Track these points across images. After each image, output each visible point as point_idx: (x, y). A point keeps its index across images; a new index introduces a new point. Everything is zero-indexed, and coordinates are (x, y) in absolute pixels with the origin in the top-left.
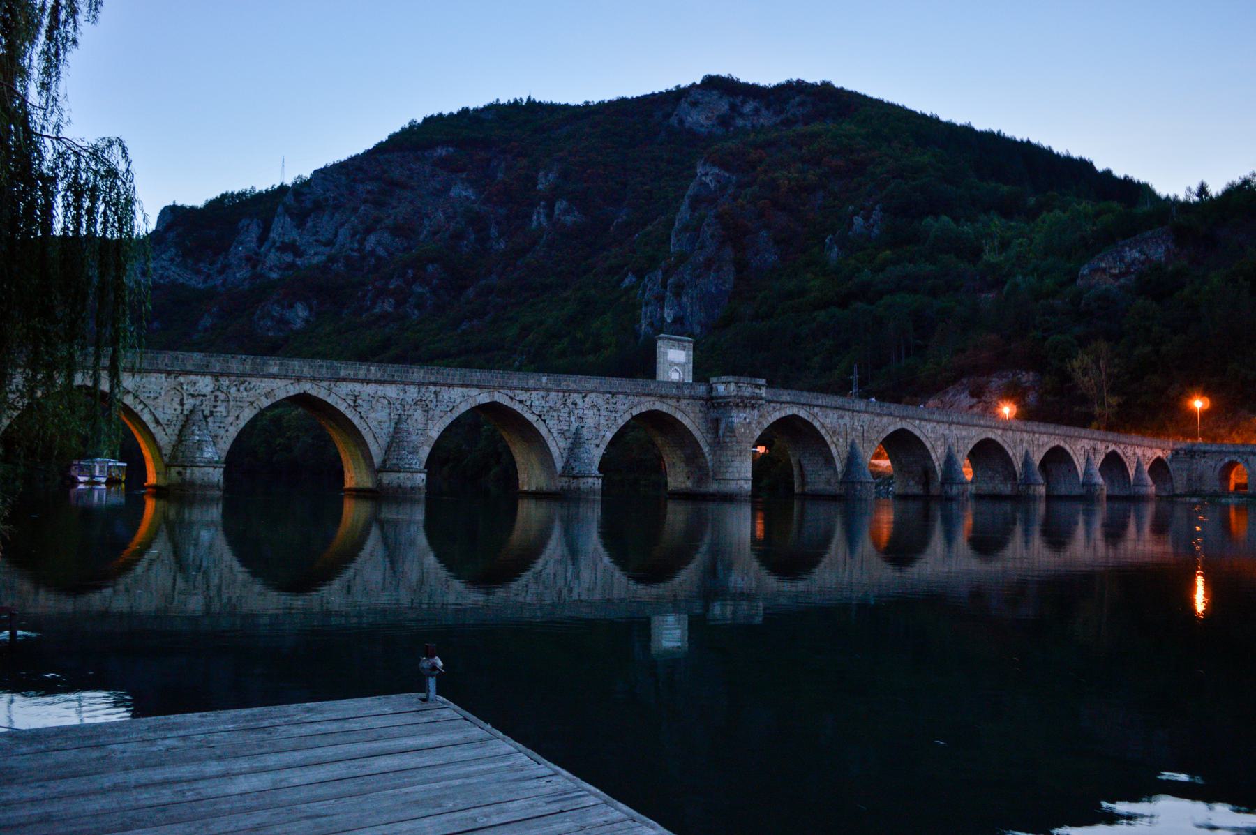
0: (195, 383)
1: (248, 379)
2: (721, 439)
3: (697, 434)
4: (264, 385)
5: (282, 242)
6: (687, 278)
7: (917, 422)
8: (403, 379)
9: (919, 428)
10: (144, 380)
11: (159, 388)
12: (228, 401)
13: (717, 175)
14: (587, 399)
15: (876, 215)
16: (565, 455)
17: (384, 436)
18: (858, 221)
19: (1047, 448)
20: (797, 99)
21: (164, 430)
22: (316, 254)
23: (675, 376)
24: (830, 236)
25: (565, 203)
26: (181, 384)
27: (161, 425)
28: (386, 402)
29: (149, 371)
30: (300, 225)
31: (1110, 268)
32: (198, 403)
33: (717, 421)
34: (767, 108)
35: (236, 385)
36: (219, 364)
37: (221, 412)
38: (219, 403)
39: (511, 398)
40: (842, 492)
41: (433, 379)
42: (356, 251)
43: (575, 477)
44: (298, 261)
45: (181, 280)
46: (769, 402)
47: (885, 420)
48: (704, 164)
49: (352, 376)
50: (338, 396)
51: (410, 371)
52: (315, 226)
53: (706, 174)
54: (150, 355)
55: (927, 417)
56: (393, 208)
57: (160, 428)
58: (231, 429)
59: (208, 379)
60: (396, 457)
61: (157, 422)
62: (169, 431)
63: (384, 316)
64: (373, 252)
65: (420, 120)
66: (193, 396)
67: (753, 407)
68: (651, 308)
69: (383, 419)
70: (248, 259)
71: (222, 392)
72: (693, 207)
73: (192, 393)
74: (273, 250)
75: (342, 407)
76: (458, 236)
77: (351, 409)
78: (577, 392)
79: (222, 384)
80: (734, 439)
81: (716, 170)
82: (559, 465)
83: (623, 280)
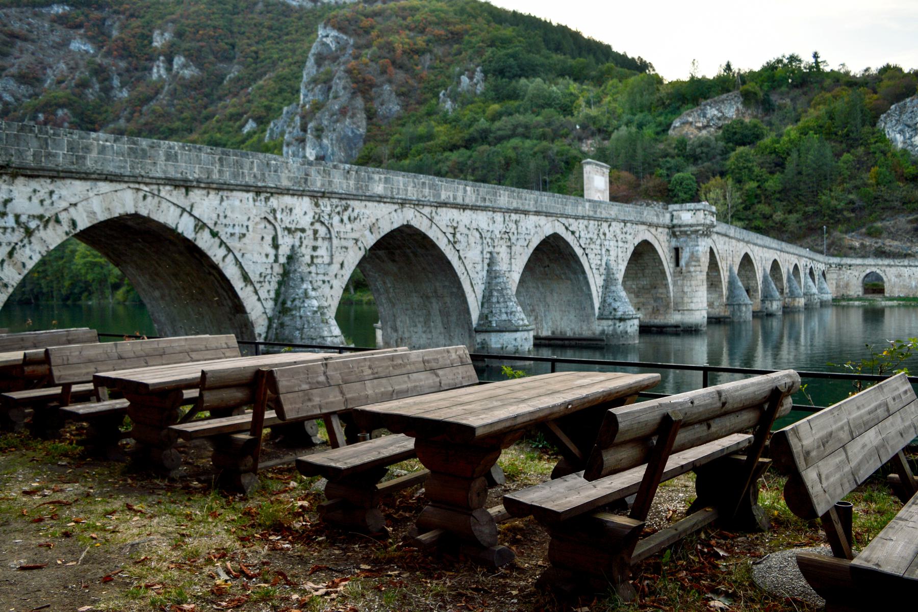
0: (291, 210)
1: (351, 203)
4: (367, 212)
6: (326, 123)
7: (752, 246)
10: (225, 204)
11: (246, 218)
12: (330, 238)
13: (337, 37)
15: (478, 76)
16: (600, 294)
18: (465, 79)
21: (256, 292)
24: (443, 92)
25: (183, 59)
26: (274, 211)
27: (252, 283)
28: (478, 235)
29: (231, 188)
32: (297, 244)
33: (677, 250)
35: (339, 213)
37: (322, 257)
38: (319, 243)
39: (567, 229)
40: (727, 314)
43: (621, 320)
47: (741, 244)
48: (325, 27)
49: (451, 200)
53: (327, 36)
54: (233, 158)
56: (15, 58)
57: (250, 289)
60: (503, 310)
61: (246, 278)
62: (263, 294)
66: (289, 230)
71: (323, 223)
73: (289, 226)
76: (84, 85)
77: (451, 246)
79: (323, 211)
81: (334, 33)
83: (243, 126)
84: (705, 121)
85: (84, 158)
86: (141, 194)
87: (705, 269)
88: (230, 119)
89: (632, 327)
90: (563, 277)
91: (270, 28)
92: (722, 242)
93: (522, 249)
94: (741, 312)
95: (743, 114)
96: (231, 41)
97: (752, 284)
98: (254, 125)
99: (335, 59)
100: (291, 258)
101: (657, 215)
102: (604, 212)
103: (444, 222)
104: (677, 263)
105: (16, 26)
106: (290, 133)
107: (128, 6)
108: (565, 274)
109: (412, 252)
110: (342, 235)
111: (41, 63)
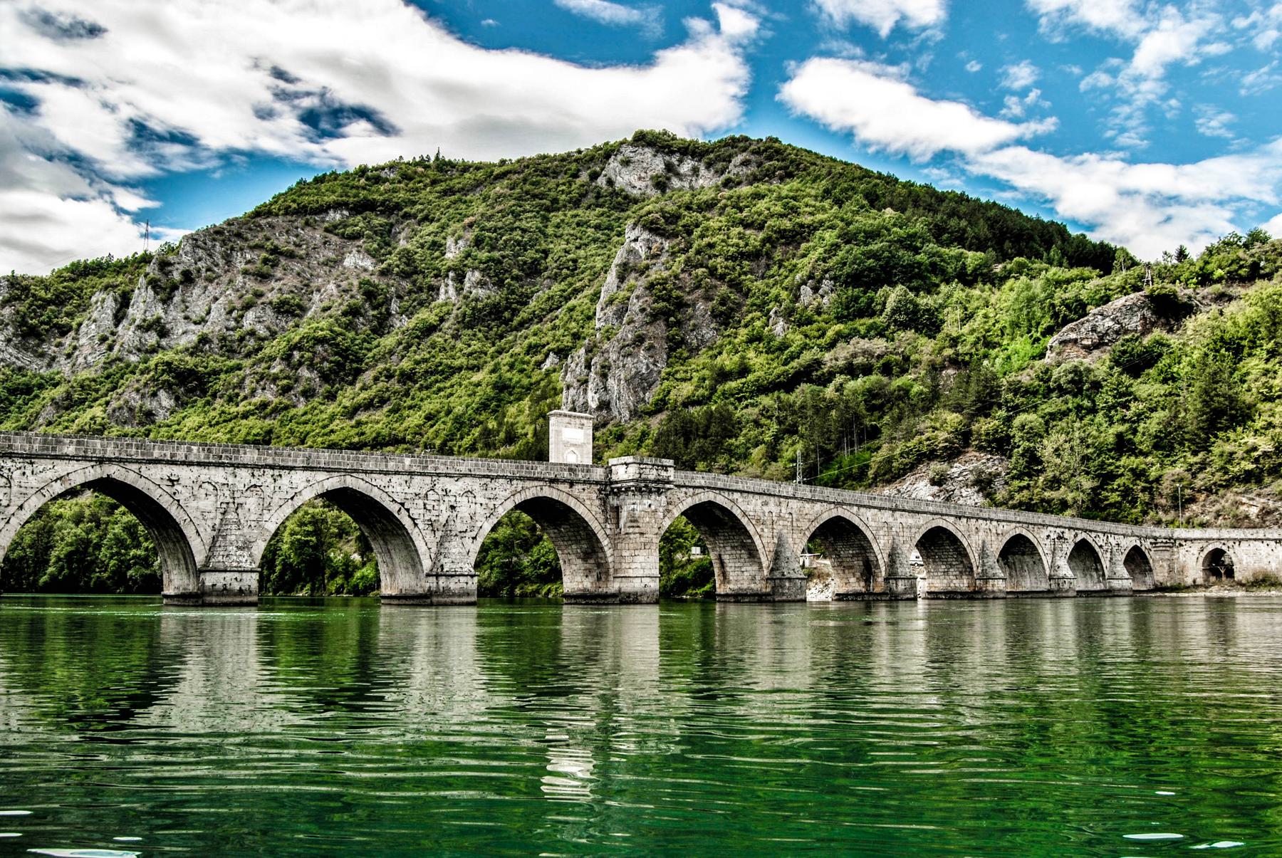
3: (595, 526)
5: (144, 320)
6: (613, 356)
8: (233, 461)
9: (857, 515)
14: (460, 483)
17: (209, 530)
18: (806, 290)
19: (1008, 537)
20: (739, 158)
22: (184, 333)
23: (572, 459)
25: (477, 274)
30: (166, 301)
31: (1082, 339)
33: (617, 510)
34: (709, 166)
41: (270, 461)
42: (233, 329)
44: (164, 342)
45: (19, 363)
46: (679, 486)
47: (818, 506)
50: (151, 480)
51: (242, 451)
52: (183, 301)
53: (636, 240)
55: (866, 503)
58: (13, 520)
63: (264, 405)
64: (252, 333)
65: (310, 180)
67: (660, 494)
68: (572, 391)
69: (208, 509)
70: (103, 339)
72: (622, 278)
74: (132, 328)
75: (155, 494)
76: (353, 312)
78: (446, 475)
80: (637, 530)
81: (646, 235)
82: (427, 564)
84: (1095, 336)
88: (527, 353)
91: (597, 227)
96: (544, 246)
98: (557, 360)
99: (643, 271)
105: (281, 241)
107: (420, 207)
111: (307, 285)
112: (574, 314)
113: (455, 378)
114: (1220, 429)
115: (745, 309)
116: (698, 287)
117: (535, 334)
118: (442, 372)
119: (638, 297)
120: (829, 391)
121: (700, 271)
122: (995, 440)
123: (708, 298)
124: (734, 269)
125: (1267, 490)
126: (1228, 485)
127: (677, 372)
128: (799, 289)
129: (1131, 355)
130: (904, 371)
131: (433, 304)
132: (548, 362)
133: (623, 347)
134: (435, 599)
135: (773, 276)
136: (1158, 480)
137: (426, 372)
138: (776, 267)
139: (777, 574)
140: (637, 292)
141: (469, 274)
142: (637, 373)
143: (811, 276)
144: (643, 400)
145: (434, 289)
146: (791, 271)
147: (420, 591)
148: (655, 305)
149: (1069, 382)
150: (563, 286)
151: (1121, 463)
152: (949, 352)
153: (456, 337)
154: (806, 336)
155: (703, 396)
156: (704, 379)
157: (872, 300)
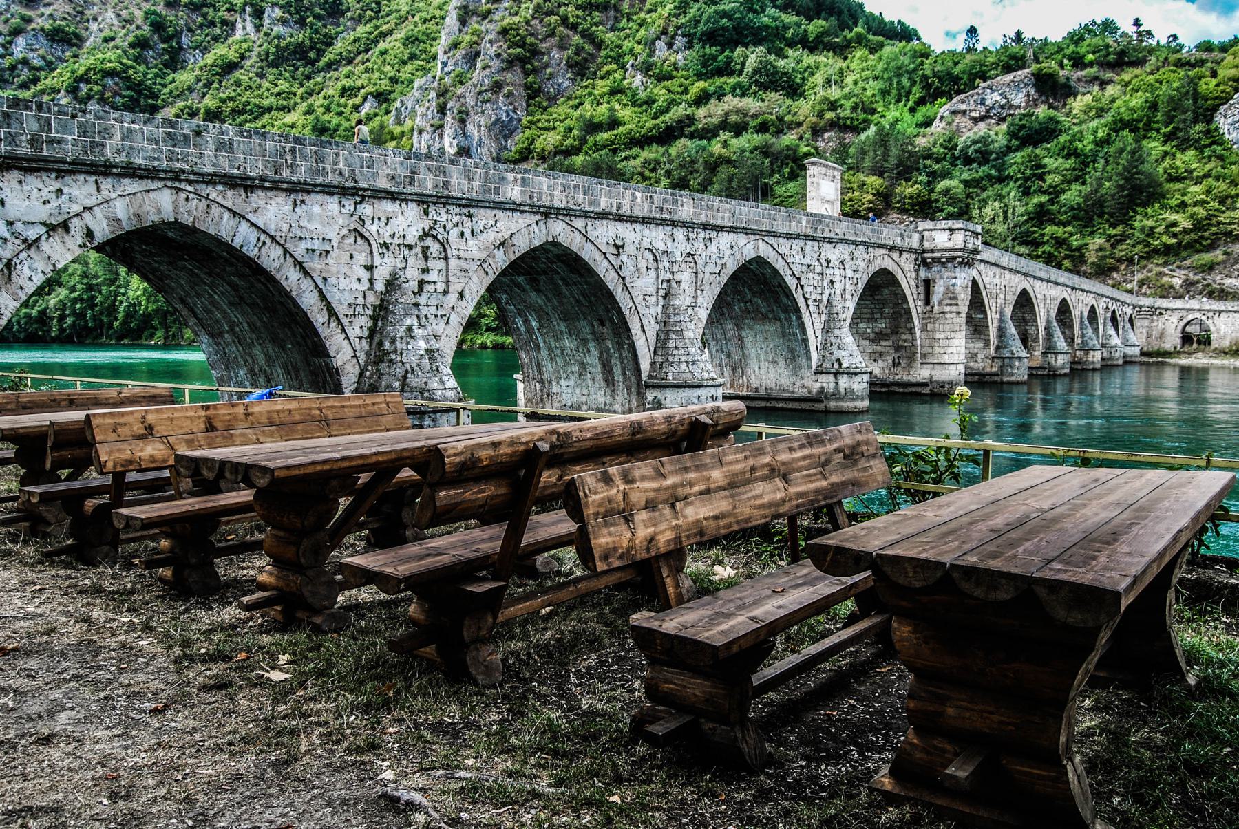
2: (936, 307)
3: (910, 301)
12: (446, 258)
14: (836, 251)
16: (819, 339)
17: (653, 322)
18: (661, 45)
25: (277, 10)
28: (651, 257)
33: (927, 283)
36: (431, 176)
38: (432, 264)
41: (703, 219)
47: (1018, 278)
49: (614, 210)
58: (455, 319)
59: (413, 210)
60: (683, 358)
68: (425, 136)
71: (435, 237)
72: (463, 22)
80: (954, 309)
84: (983, 109)
85: (103, 145)
86: (183, 195)
87: (964, 308)
88: (342, 95)
89: (860, 385)
90: (770, 316)
92: (991, 274)
93: (712, 278)
94: (1012, 367)
95: (1035, 101)
97: (1031, 330)
99: (485, 16)
100: (392, 283)
101: (902, 235)
102: (827, 230)
103: (605, 240)
104: (927, 301)
106: (423, 116)
108: (773, 311)
109: (563, 279)
110: (462, 254)
112: (388, 57)
113: (266, 118)
114: (1138, 205)
115: (599, 60)
116: (552, 34)
117: (347, 77)
118: (251, 112)
119: (491, 42)
120: (716, 148)
121: (553, 19)
122: (919, 203)
123: (562, 47)
124: (585, 19)
125: (1188, 263)
126: (1148, 256)
127: (538, 121)
128: (653, 43)
129: (1030, 129)
130: (779, 132)
131: (230, 40)
132: (367, 105)
133: (480, 93)
134: (832, 405)
135: (623, 29)
136: (1079, 249)
137: (233, 111)
138: (625, 20)
139: (1006, 353)
140: (490, 37)
141: (268, 10)
142: (497, 120)
143: (665, 32)
144: (505, 148)
145: (229, 26)
146: (641, 25)
147: (800, 392)
148: (511, 51)
149: (976, 151)
150: (368, 28)
151: (1046, 231)
152: (829, 115)
153: (261, 76)
154: (669, 91)
155: (572, 146)
156: (570, 129)
157: (730, 60)
